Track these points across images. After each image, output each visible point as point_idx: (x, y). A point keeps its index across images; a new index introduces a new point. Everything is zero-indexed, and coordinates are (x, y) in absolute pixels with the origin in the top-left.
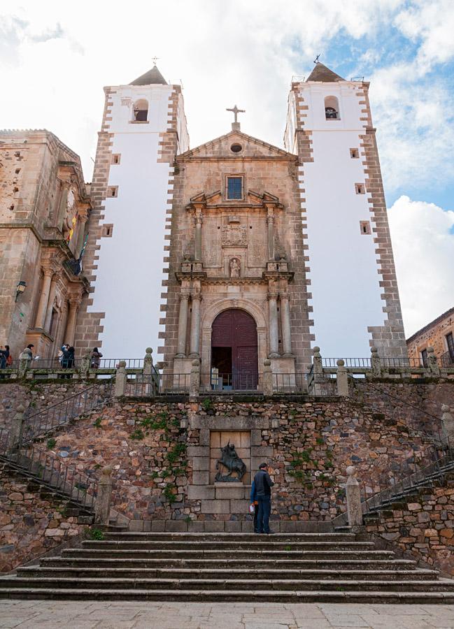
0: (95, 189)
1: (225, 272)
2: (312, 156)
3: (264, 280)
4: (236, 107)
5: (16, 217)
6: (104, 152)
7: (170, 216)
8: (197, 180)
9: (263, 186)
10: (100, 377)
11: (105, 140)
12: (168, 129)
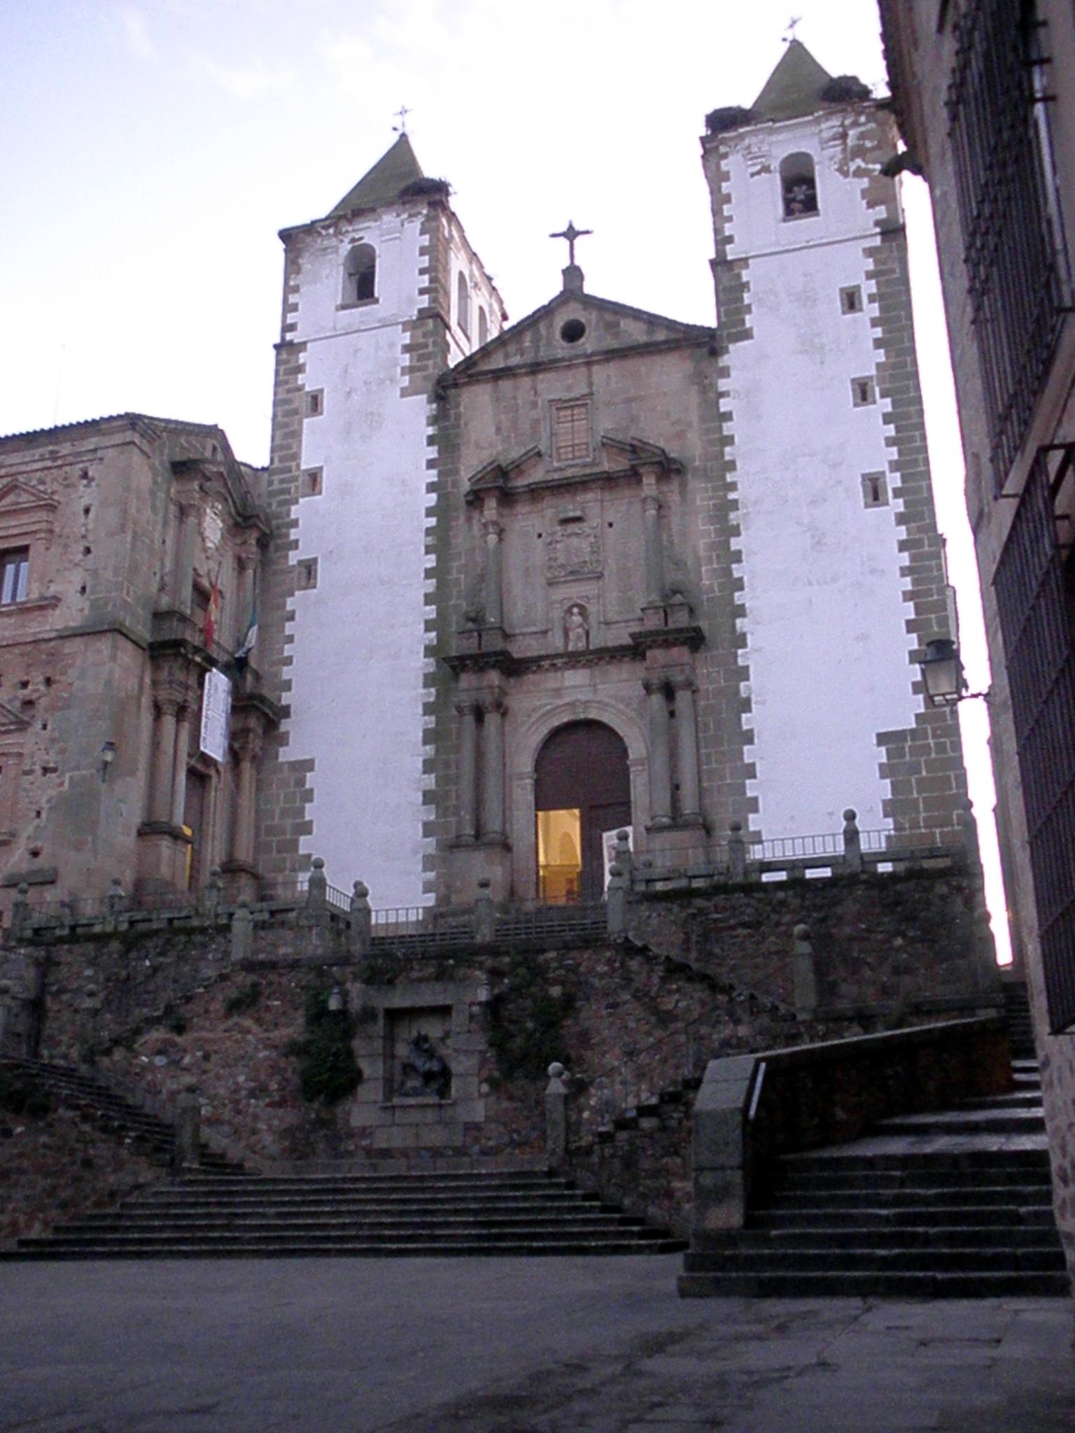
0: (276, 483)
1: (556, 642)
4: (571, 227)
6: (288, 391)
7: (432, 521)
8: (487, 427)
9: (634, 420)
12: (420, 311)
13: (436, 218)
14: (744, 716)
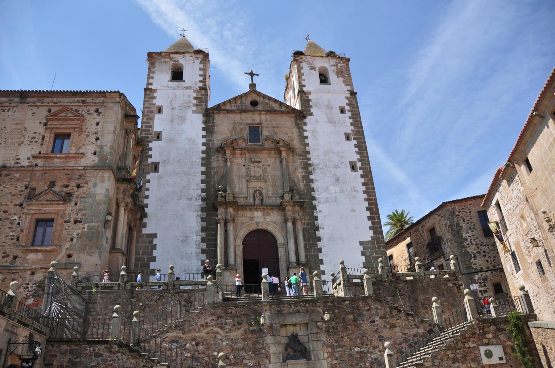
2: (312, 111)
3: (281, 207)
4: (252, 72)
5: (99, 160)
6: (149, 104)
7: (204, 156)
8: (225, 127)
9: (276, 134)
10: (182, 287)
11: (149, 95)
12: (200, 87)
13: (206, 60)
14: (317, 232)
